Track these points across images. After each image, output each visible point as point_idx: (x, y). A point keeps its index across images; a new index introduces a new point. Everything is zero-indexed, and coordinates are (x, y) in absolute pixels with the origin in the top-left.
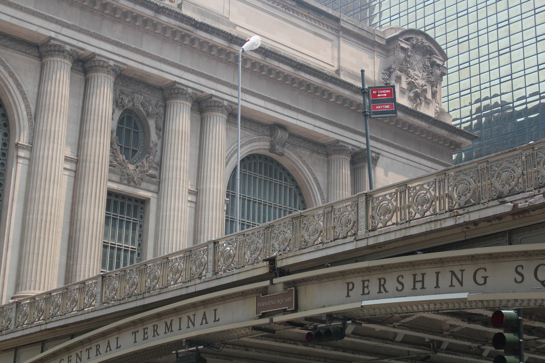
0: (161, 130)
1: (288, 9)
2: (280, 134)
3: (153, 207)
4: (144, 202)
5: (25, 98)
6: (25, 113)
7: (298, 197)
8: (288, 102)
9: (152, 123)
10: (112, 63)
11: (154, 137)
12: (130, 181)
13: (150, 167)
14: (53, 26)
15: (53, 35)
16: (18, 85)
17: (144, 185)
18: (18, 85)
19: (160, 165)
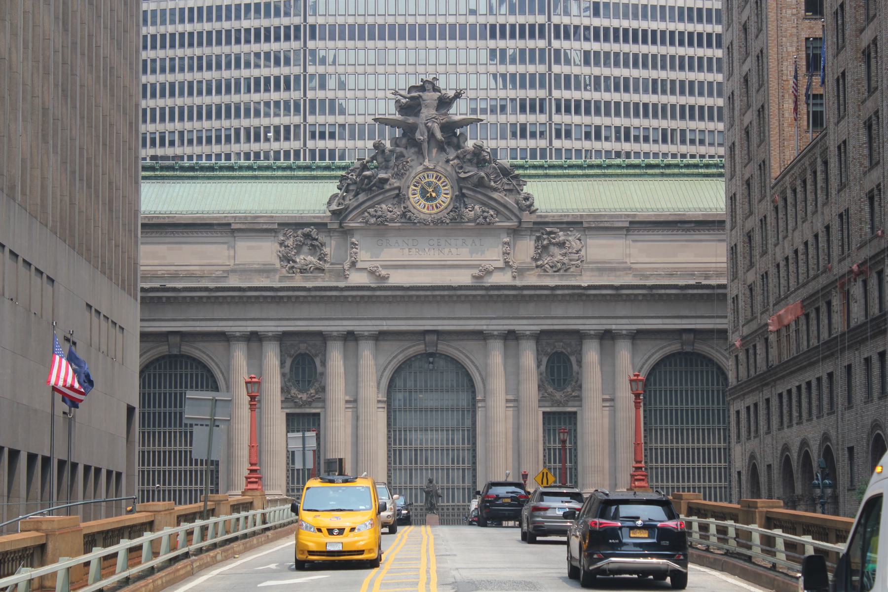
0: (580, 362)
1: (688, 230)
2: (685, 336)
3: (579, 416)
4: (575, 413)
5: (478, 369)
6: (479, 378)
7: (721, 377)
8: (686, 313)
9: (573, 359)
10: (528, 333)
11: (575, 367)
12: (559, 403)
13: (573, 391)
14: (484, 322)
15: (485, 328)
16: (472, 362)
17: (570, 403)
18: (472, 362)
19: (580, 387)
